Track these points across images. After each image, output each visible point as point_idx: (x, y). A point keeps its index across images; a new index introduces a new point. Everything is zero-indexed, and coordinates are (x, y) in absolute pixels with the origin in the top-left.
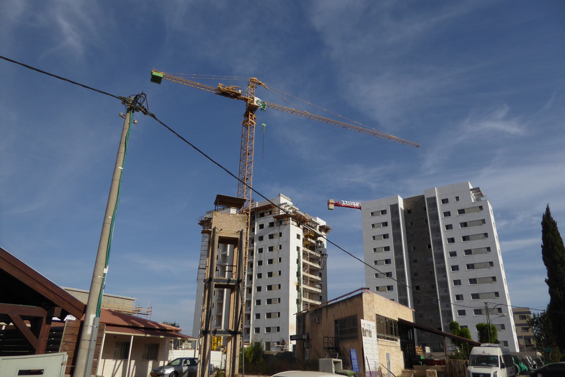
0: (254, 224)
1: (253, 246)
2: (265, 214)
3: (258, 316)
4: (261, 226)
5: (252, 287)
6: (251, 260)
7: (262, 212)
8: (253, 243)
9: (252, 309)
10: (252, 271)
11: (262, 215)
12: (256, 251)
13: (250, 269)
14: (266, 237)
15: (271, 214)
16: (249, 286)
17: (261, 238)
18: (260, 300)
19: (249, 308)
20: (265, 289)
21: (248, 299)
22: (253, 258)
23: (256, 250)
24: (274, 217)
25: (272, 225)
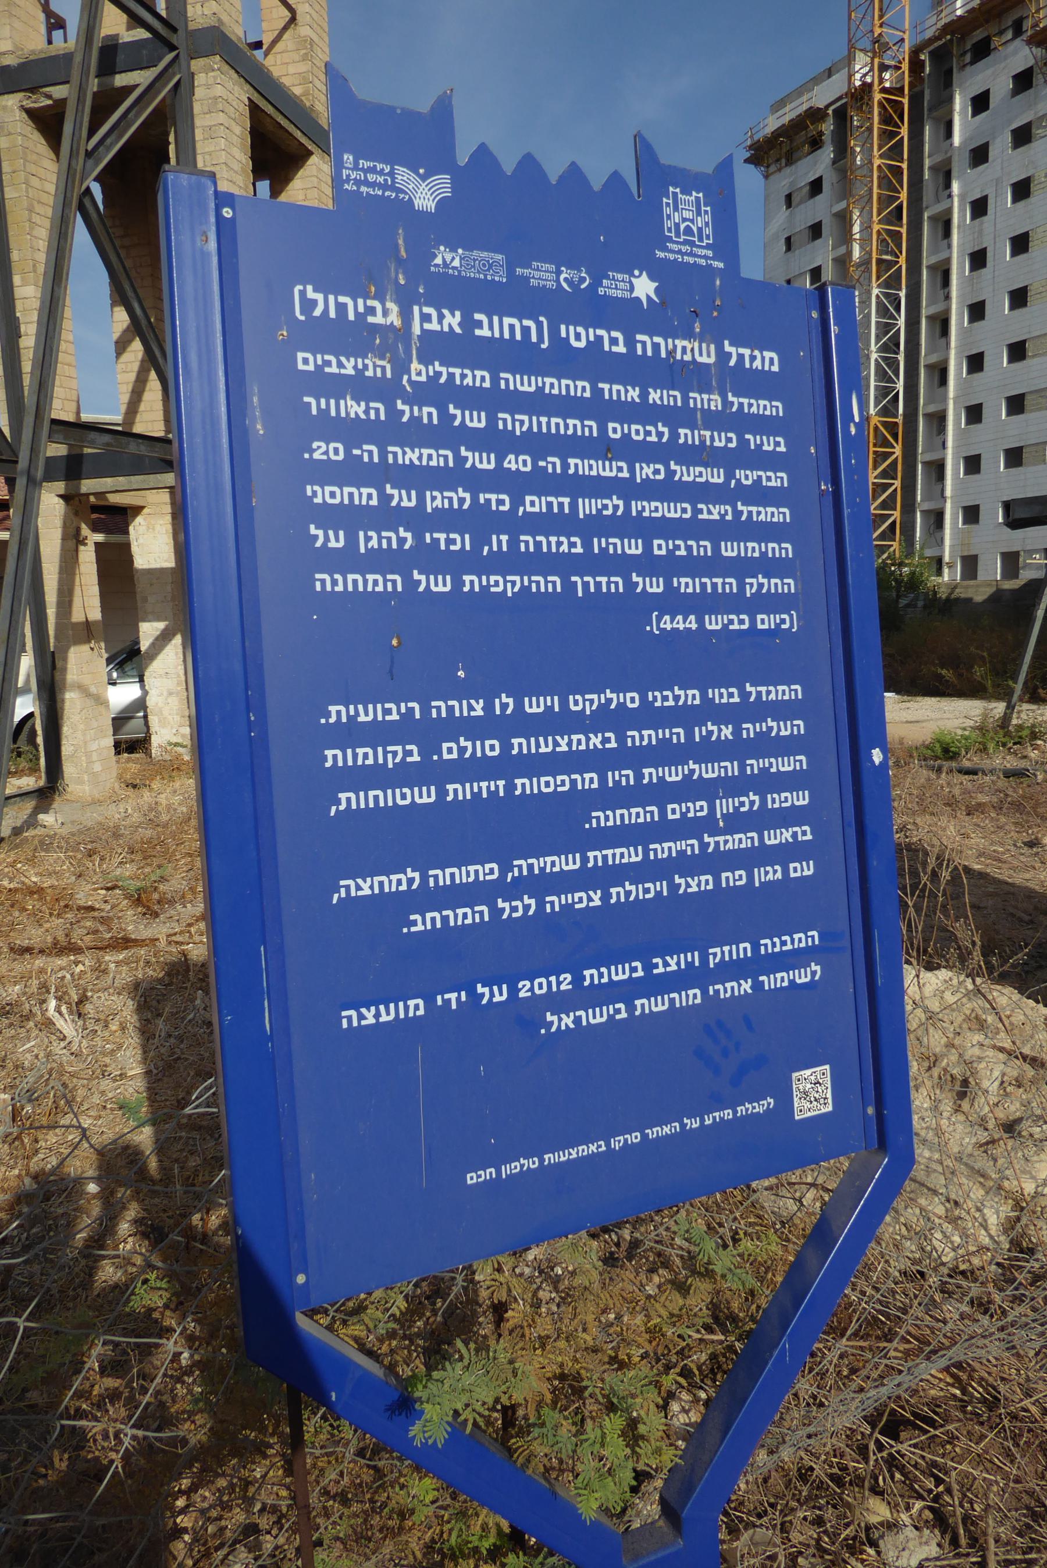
0: (950, 100)
1: (950, 196)
2: (996, 41)
3: (973, 464)
4: (980, 103)
5: (946, 361)
6: (942, 256)
7: (978, 35)
8: (948, 185)
9: (950, 443)
10: (948, 297)
11: (982, 51)
12: (960, 215)
13: (941, 294)
14: (1001, 146)
15: (1018, 31)
16: (934, 359)
17: (979, 155)
18: (979, 407)
19: (938, 441)
20: (998, 360)
21: (931, 409)
22: (950, 246)
23: (962, 211)
24: (1030, 42)
25: (1023, 81)
